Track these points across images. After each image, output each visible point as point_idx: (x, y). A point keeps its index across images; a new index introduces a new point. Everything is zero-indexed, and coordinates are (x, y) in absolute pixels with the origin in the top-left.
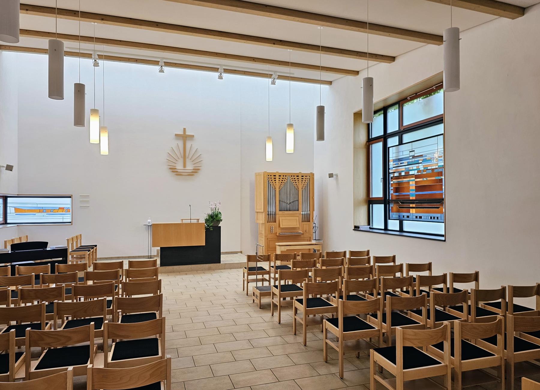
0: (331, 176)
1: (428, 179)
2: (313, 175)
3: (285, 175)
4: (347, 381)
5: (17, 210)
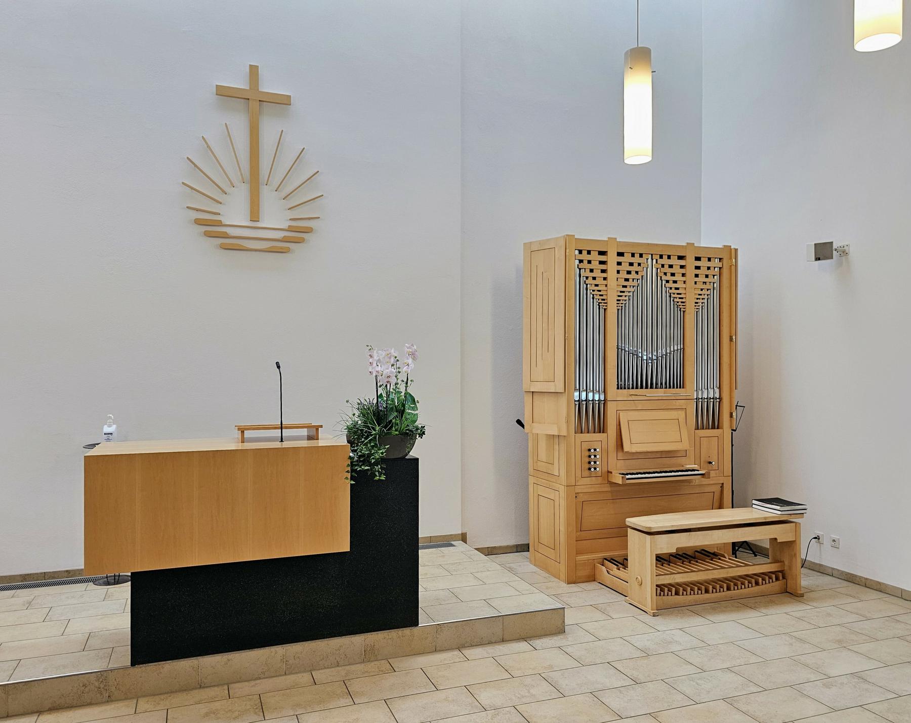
0: (823, 252)
3: (630, 256)
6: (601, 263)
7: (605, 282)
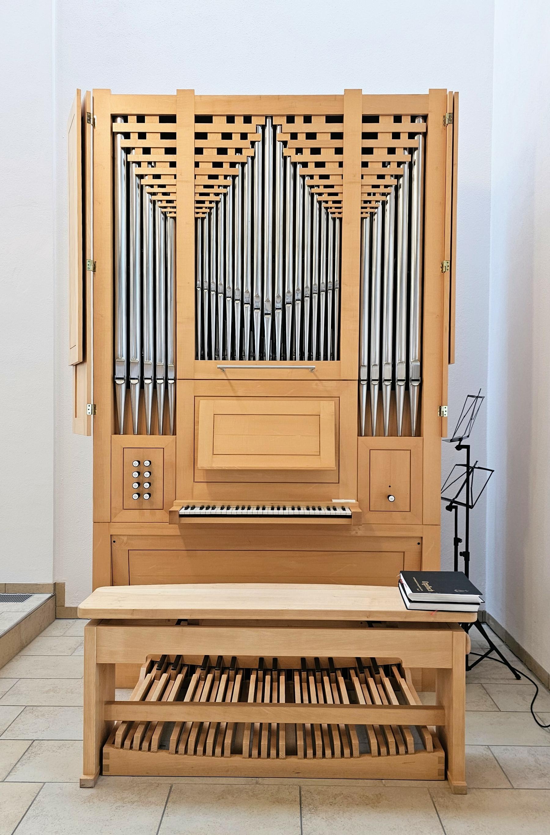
6: (165, 136)
7: (173, 171)
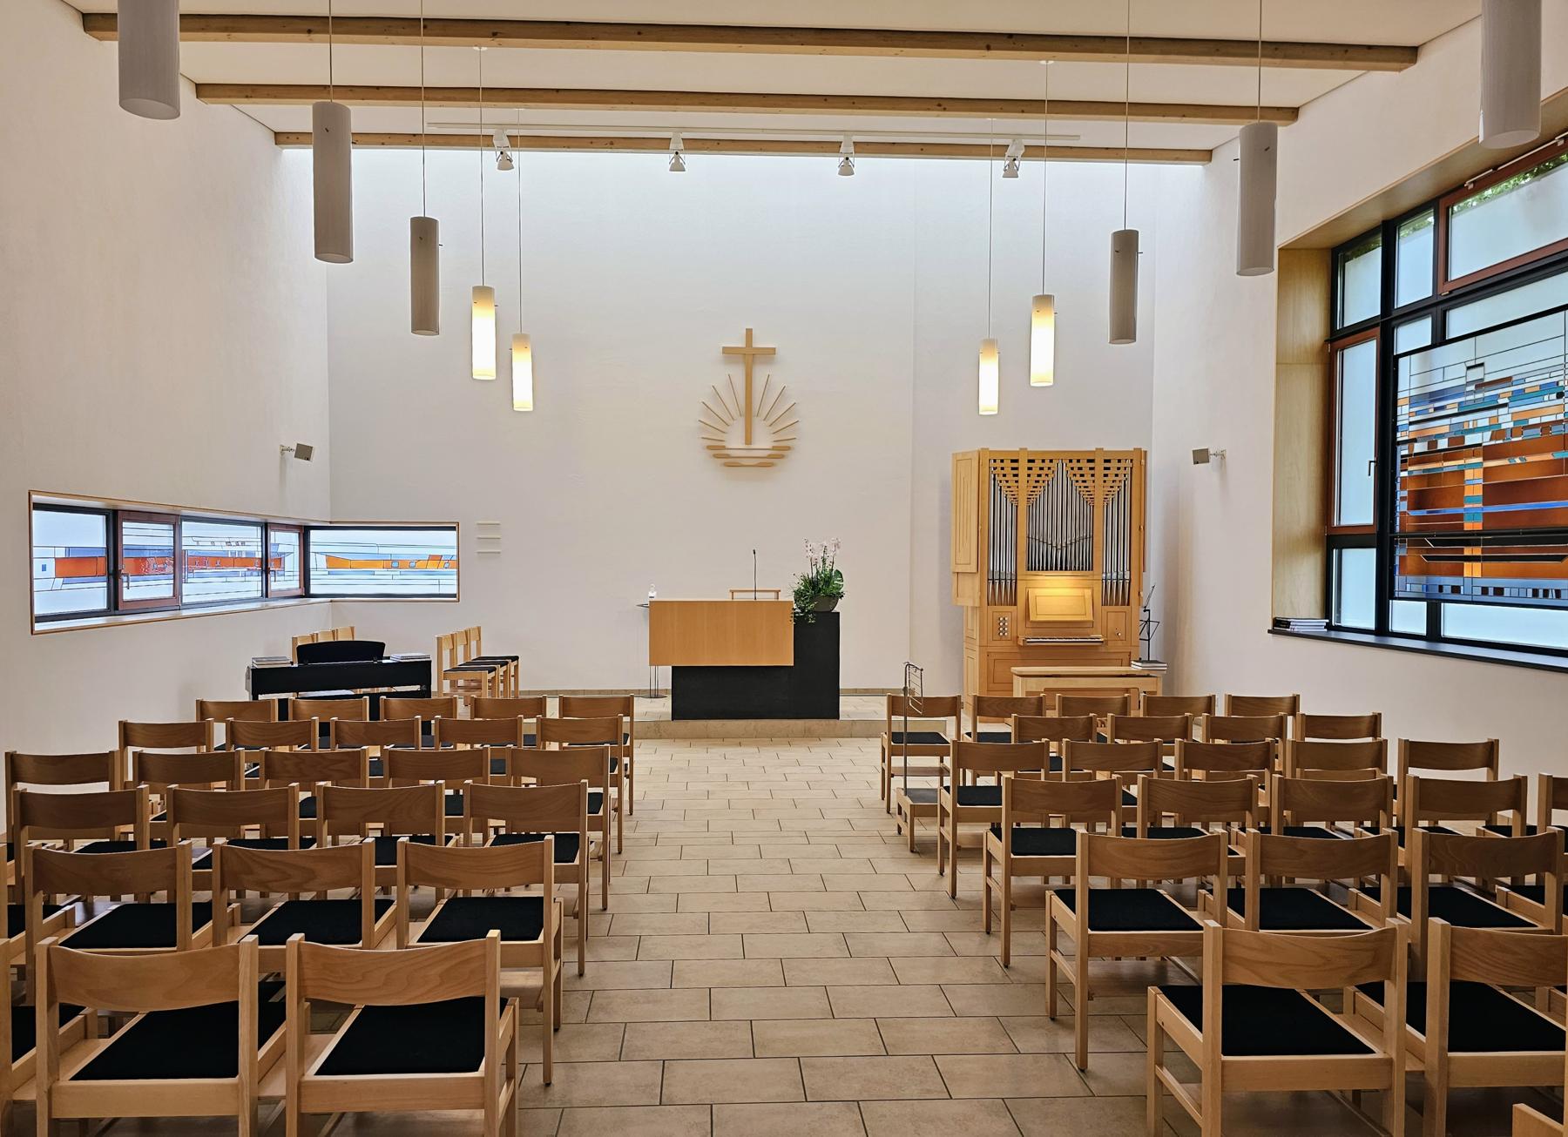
0: (1201, 457)
1: (1530, 459)
2: (1142, 455)
3: (1049, 458)
4: (1096, 1078)
5: (334, 562)
